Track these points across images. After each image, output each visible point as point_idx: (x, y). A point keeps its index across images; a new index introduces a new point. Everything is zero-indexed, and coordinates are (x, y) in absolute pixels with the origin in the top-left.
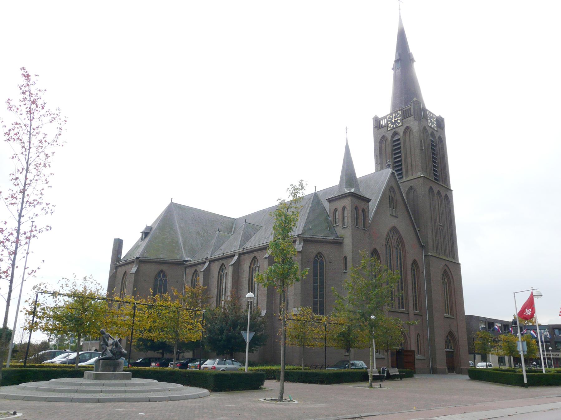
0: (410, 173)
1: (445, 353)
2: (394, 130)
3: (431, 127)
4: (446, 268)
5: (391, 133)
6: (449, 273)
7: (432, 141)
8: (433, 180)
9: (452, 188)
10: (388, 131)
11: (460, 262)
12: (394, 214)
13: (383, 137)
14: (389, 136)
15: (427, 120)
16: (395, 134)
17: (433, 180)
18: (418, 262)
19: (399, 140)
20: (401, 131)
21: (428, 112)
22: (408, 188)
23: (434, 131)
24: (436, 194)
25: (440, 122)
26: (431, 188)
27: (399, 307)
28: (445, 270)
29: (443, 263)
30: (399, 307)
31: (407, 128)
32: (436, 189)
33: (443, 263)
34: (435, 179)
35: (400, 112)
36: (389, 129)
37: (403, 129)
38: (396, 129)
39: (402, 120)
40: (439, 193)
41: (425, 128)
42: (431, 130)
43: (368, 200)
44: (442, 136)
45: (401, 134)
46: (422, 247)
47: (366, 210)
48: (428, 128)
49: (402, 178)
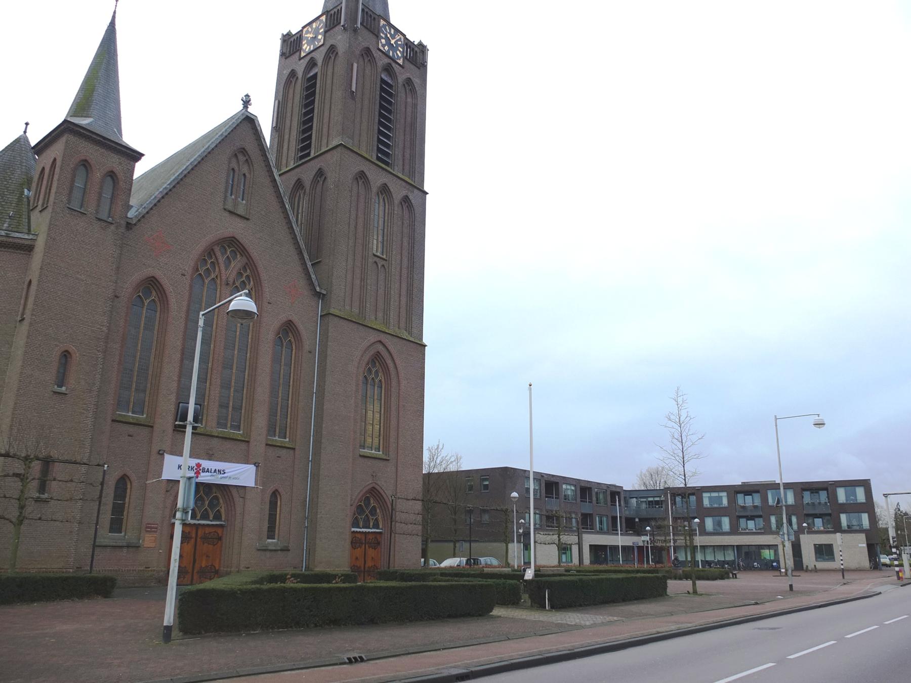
0: (324, 141)
1: (348, 538)
2: (308, 58)
3: (386, 55)
4: (380, 348)
5: (304, 62)
6: (389, 362)
7: (383, 81)
8: (374, 159)
9: (426, 189)
10: (300, 59)
11: (425, 340)
12: (240, 211)
13: (293, 74)
14: (300, 67)
15: (378, 37)
16: (312, 63)
17: (374, 159)
18: (301, 327)
19: (315, 75)
20: (319, 57)
21: (382, 22)
22: (314, 173)
23: (394, 65)
24: (396, 202)
25: (417, 55)
26: (361, 176)
27: (219, 424)
28: (378, 355)
29: (373, 337)
30: (219, 424)
31: (332, 49)
32: (377, 178)
33: (373, 337)
34: (378, 158)
35: (324, 18)
36: (303, 54)
37: (324, 50)
38: (313, 55)
39: (326, 32)
40: (384, 190)
41: (367, 51)
42: (387, 60)
43: (136, 156)
44: (416, 81)
45: (320, 63)
46: (319, 295)
47: (121, 176)
48: (376, 54)
49: (309, 154)
